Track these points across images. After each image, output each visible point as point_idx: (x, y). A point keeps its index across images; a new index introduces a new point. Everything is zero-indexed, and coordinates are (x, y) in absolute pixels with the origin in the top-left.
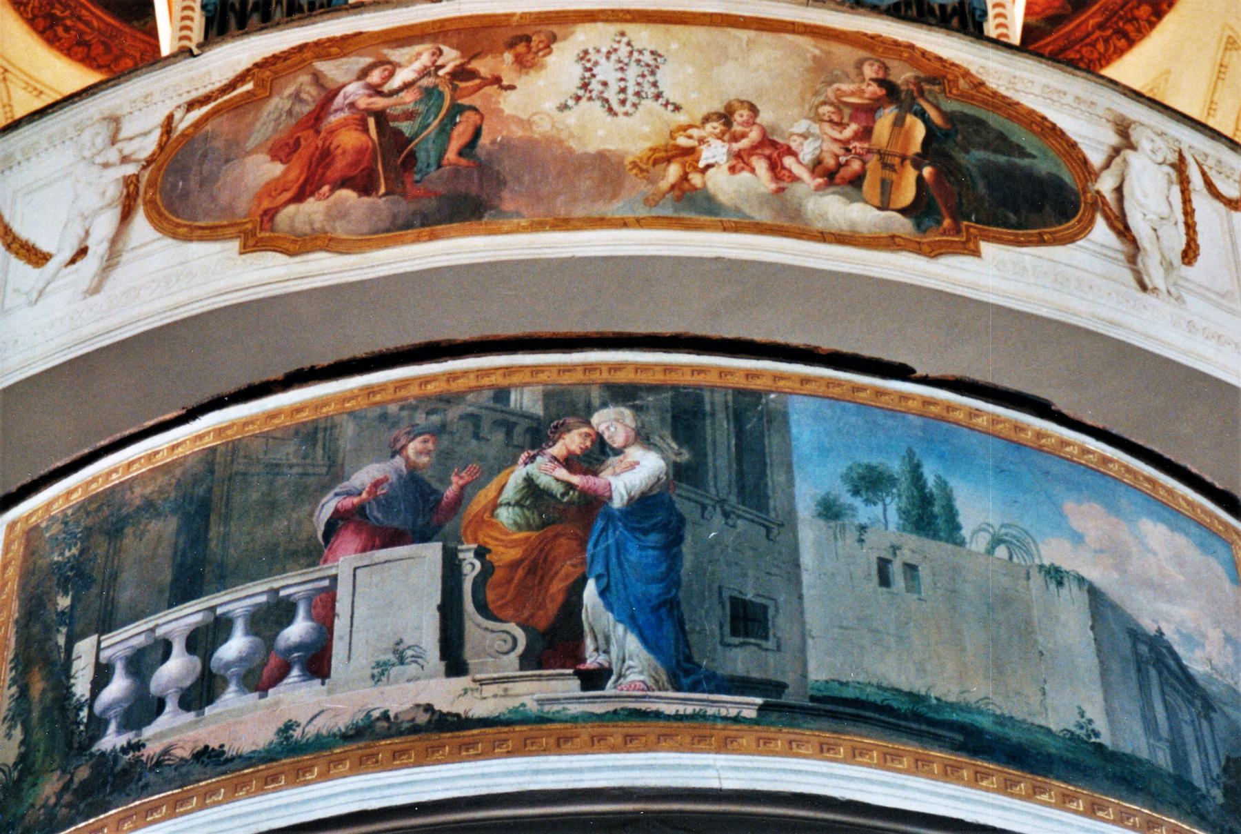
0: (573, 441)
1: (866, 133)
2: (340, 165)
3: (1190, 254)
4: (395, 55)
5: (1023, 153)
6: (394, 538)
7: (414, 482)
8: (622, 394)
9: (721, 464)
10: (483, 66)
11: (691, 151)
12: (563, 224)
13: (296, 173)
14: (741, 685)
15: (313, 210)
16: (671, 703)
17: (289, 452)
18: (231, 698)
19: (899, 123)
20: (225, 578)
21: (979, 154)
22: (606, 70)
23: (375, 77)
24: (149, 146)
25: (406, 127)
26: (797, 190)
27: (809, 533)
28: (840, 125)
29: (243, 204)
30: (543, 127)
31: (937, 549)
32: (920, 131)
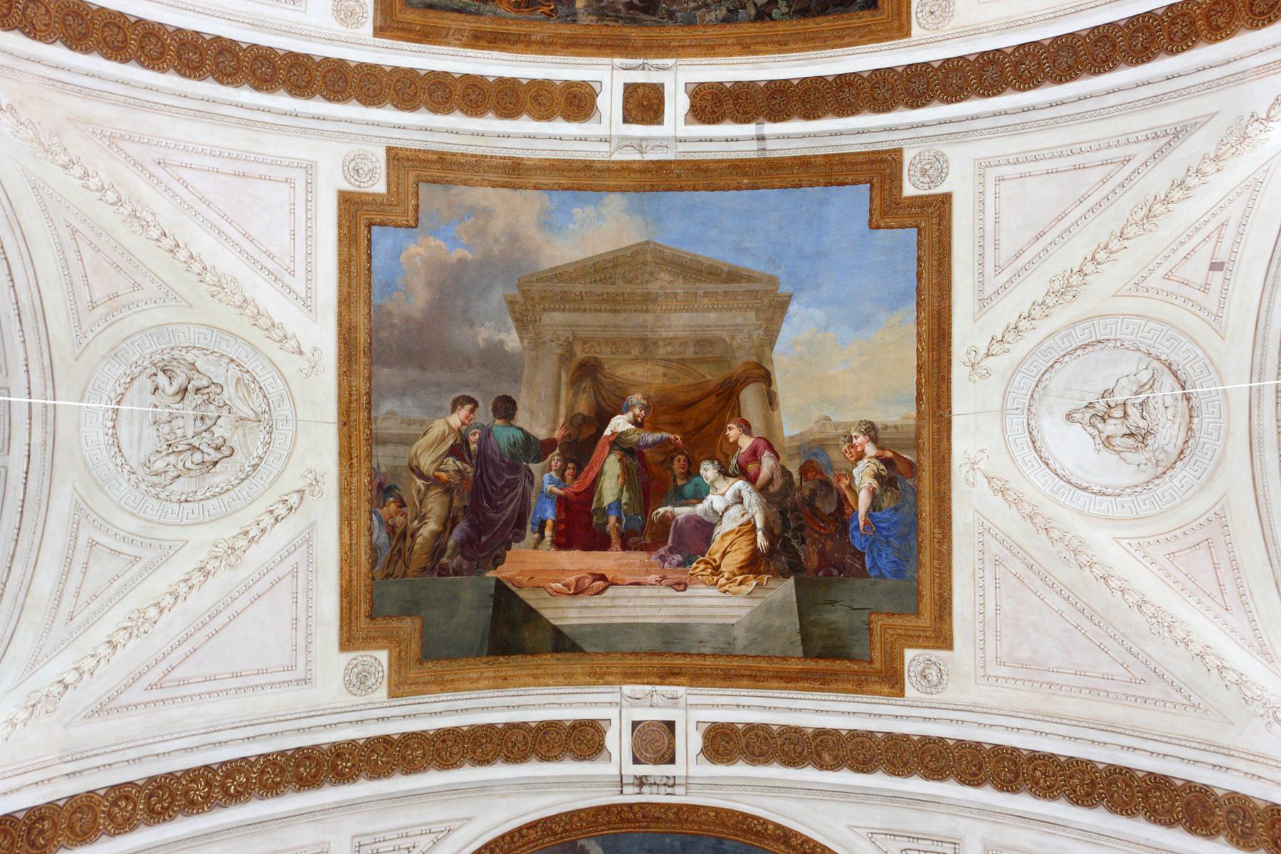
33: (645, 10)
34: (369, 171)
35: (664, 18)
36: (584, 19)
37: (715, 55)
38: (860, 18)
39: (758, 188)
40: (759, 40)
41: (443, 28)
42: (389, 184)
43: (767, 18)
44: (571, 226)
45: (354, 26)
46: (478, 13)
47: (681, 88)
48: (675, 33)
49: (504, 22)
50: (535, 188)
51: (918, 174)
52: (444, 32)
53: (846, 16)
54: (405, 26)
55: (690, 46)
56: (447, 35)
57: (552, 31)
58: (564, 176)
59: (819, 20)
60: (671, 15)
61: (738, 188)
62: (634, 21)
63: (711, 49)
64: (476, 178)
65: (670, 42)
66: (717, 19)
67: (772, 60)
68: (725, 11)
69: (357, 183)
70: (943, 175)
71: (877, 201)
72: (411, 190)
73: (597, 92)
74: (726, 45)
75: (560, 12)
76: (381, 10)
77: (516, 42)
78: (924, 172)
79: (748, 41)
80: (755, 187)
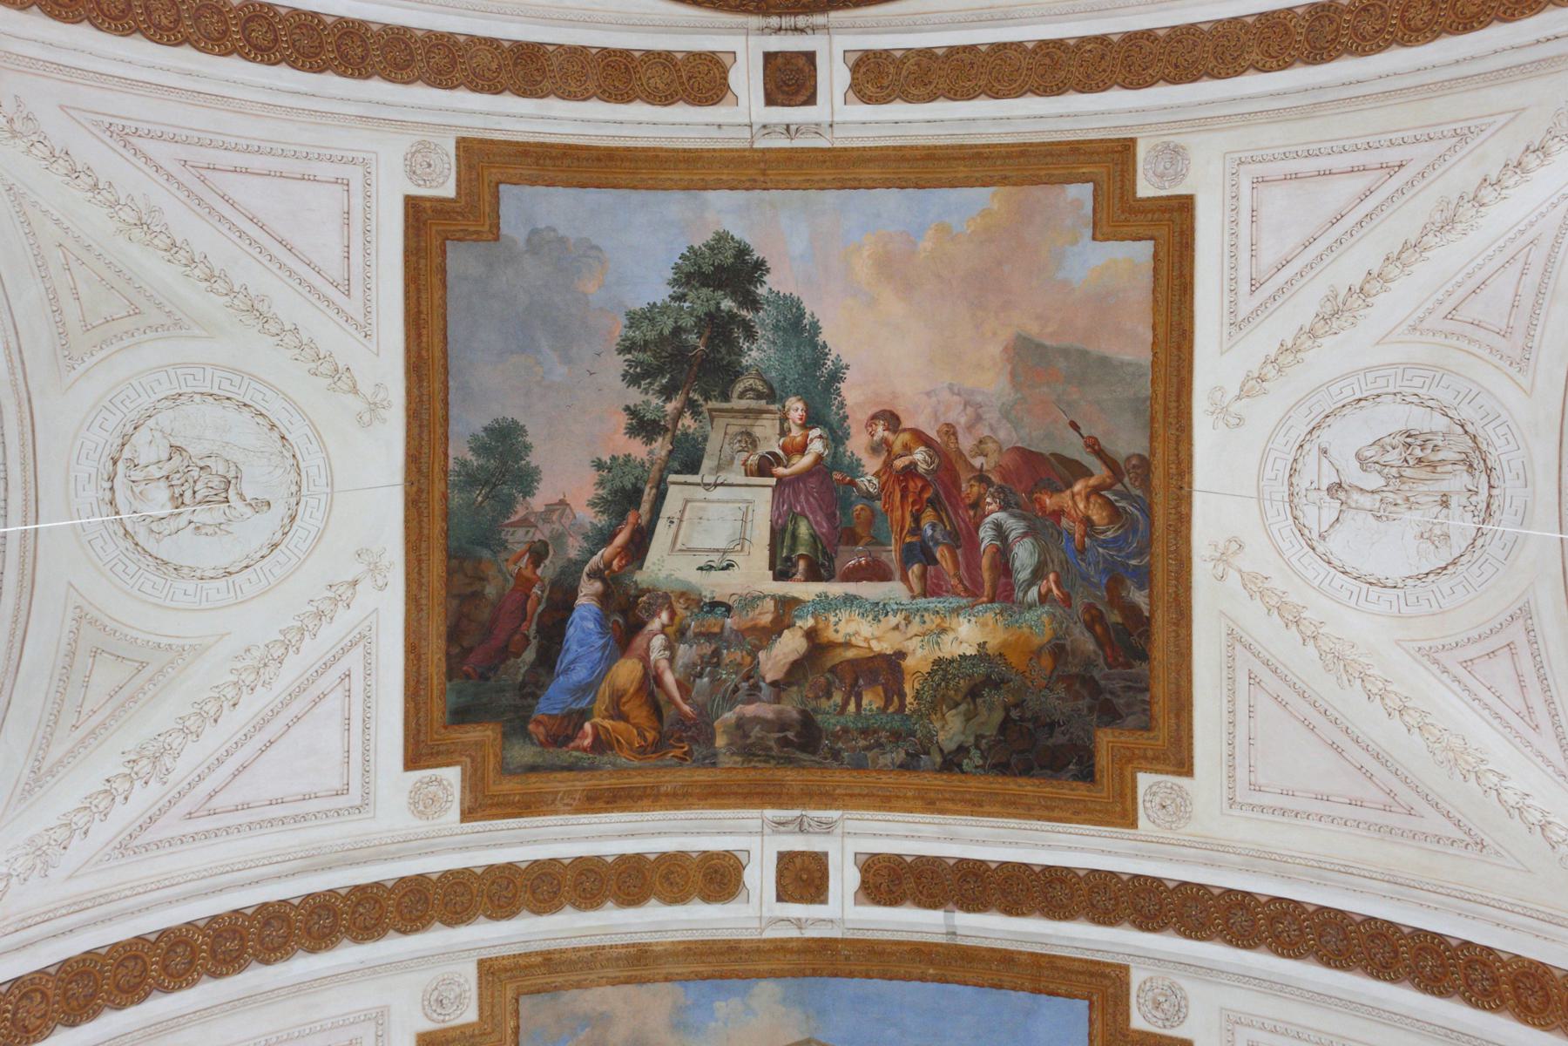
33: (803, 748)
34: (456, 998)
35: (826, 758)
36: (726, 760)
37: (891, 809)
38: (1073, 790)
39: (947, 982)
40: (947, 796)
41: (546, 793)
42: (481, 1008)
43: (957, 769)
44: (713, 1024)
45: (436, 816)
46: (592, 768)
47: (850, 859)
48: (840, 778)
49: (625, 775)
50: (667, 979)
51: (1150, 1004)
52: (550, 797)
53: (1055, 782)
54: (501, 799)
55: (859, 795)
56: (553, 802)
57: (687, 779)
58: (703, 962)
59: (1021, 780)
60: (836, 755)
61: (922, 979)
62: (790, 761)
63: (885, 801)
64: (592, 977)
65: (834, 790)
66: (893, 764)
67: (963, 823)
68: (903, 754)
69: (441, 1018)
70: (1182, 1015)
71: (1098, 1025)
72: (510, 1008)
73: (744, 864)
74: (905, 797)
75: (696, 753)
76: (470, 787)
77: (640, 798)
78: (1157, 1005)
79: (932, 795)
80: (943, 980)
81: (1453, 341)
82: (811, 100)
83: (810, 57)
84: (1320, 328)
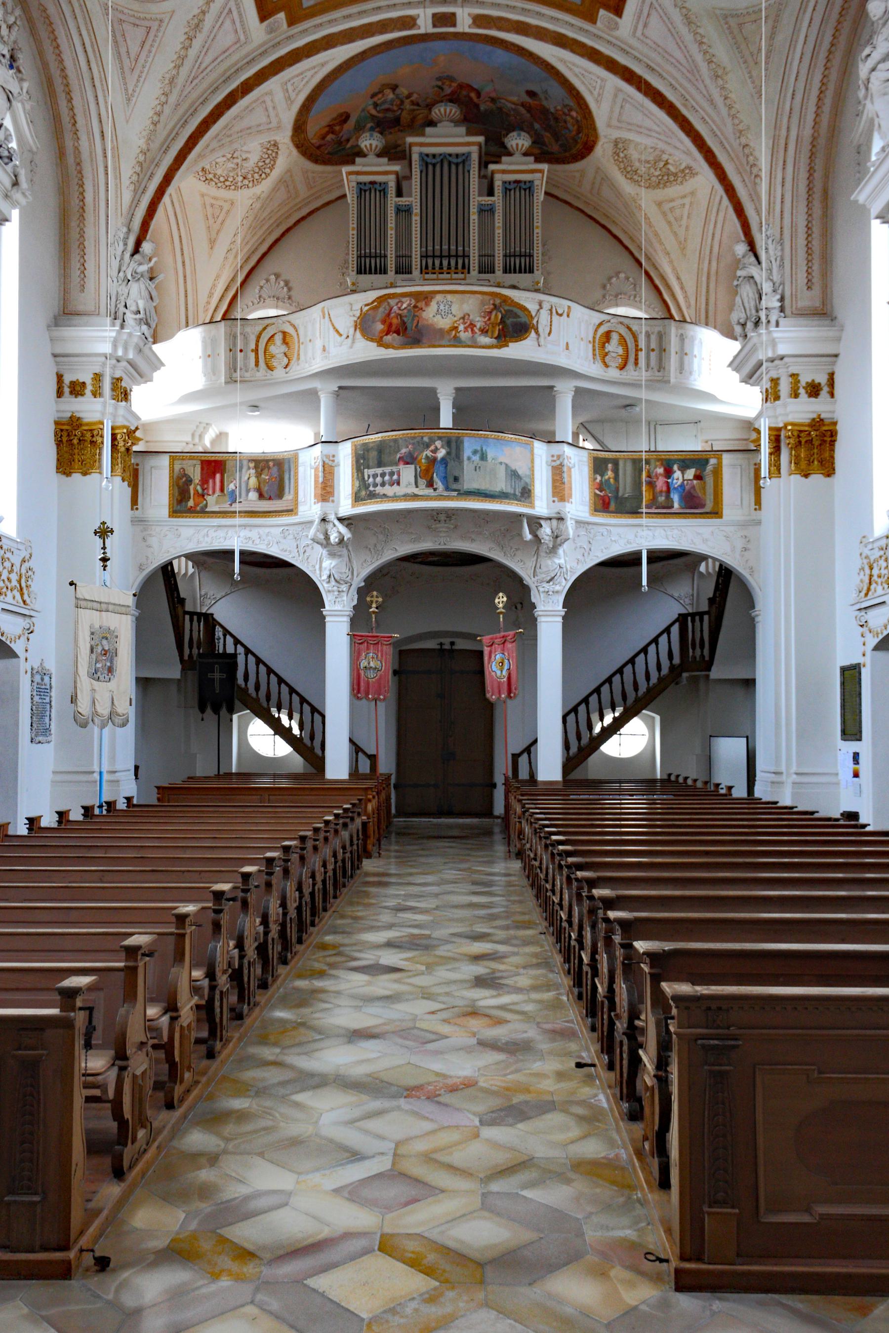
0: (432, 448)
1: (489, 319)
2: (394, 328)
3: (549, 334)
4: (404, 300)
5: (519, 317)
6: (408, 463)
7: (410, 454)
8: (440, 438)
9: (454, 451)
10: (419, 305)
11: (457, 328)
12: (434, 346)
13: (386, 328)
14: (455, 490)
15: (388, 339)
16: (446, 494)
17: (392, 444)
18: (387, 487)
19: (496, 315)
20: (385, 466)
21: (511, 320)
22: (442, 307)
23: (399, 305)
24: (358, 314)
25: (405, 319)
26: (476, 336)
27: (466, 462)
28: (484, 317)
29: (377, 334)
30: (430, 322)
31: (483, 462)
32: (500, 316)
81: (142, 16)
82: (434, 15)
83: (434, 26)
84: (201, 17)
